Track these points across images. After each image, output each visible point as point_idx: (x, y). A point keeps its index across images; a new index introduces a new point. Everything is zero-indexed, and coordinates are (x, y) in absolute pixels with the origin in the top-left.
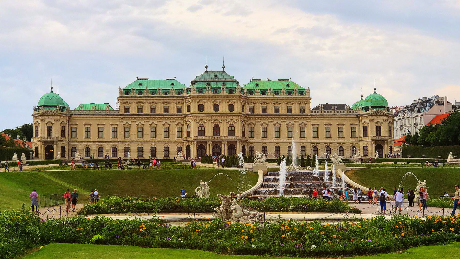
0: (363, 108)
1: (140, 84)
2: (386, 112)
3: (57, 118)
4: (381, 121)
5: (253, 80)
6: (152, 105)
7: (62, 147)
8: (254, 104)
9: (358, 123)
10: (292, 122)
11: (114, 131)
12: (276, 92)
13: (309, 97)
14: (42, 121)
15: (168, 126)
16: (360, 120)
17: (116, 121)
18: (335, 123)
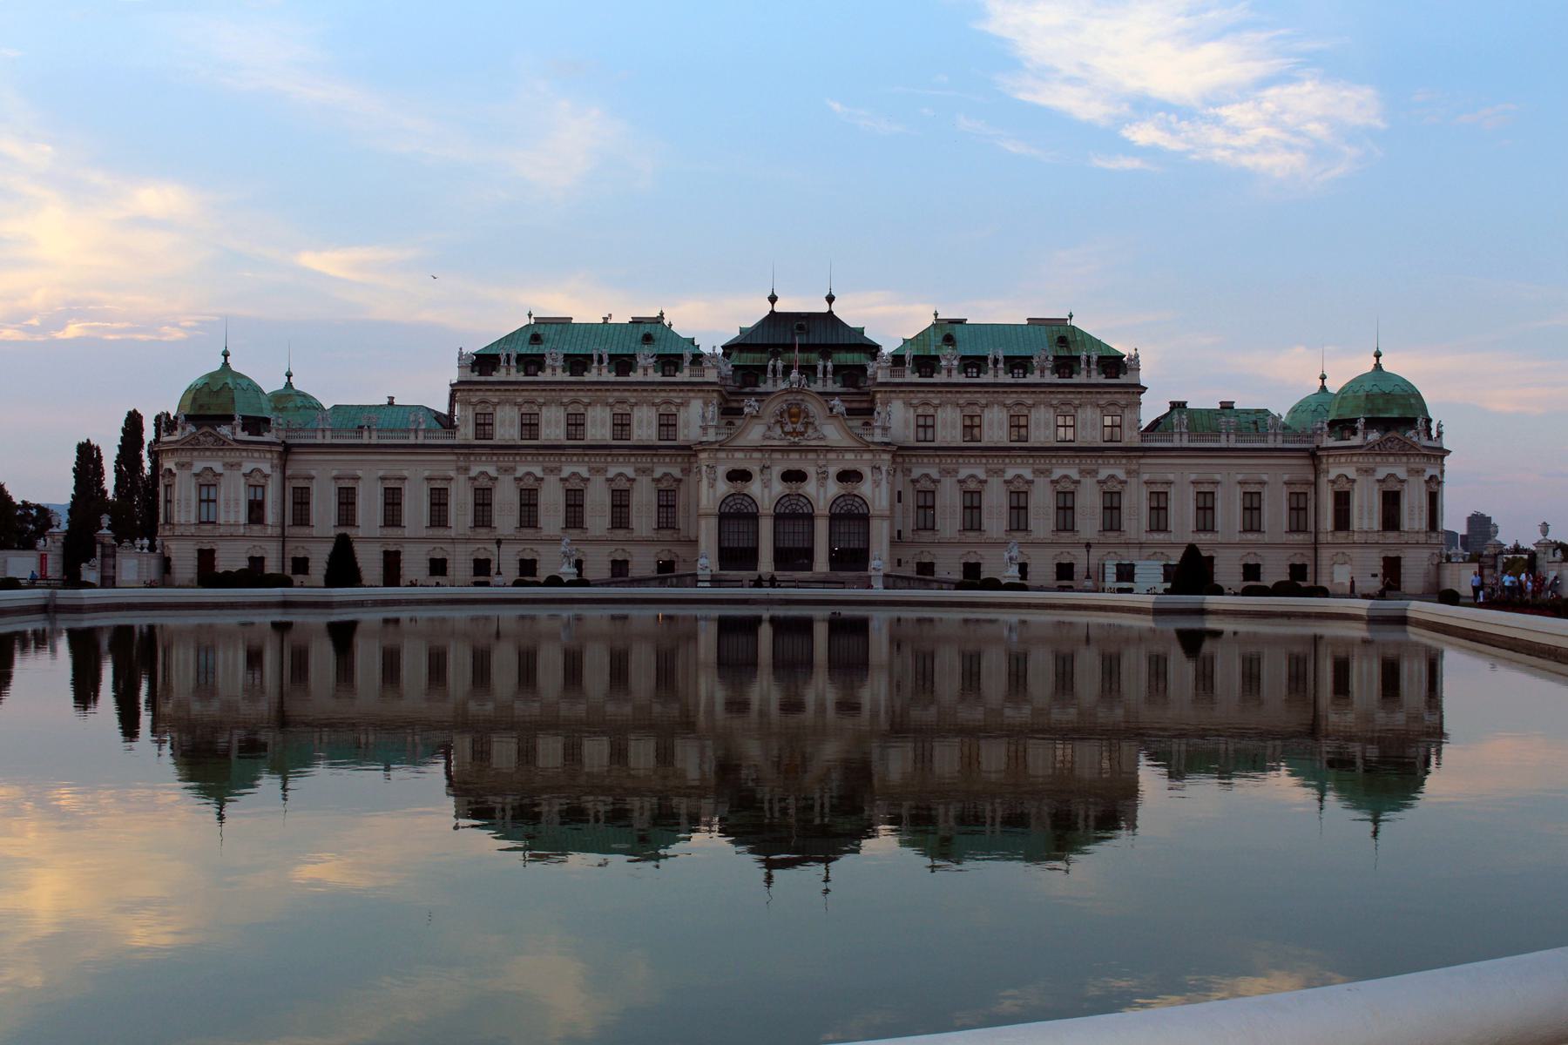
0: (1332, 424)
1: (536, 339)
2: (1425, 442)
3: (232, 457)
4: (1401, 472)
5: (939, 324)
6: (570, 410)
7: (251, 559)
8: (936, 407)
9: (1312, 478)
10: (1076, 477)
11: (439, 501)
12: (1018, 363)
13: (1138, 386)
14: (181, 466)
15: (627, 485)
16: (1324, 466)
17: (445, 466)
18: (1229, 480)
